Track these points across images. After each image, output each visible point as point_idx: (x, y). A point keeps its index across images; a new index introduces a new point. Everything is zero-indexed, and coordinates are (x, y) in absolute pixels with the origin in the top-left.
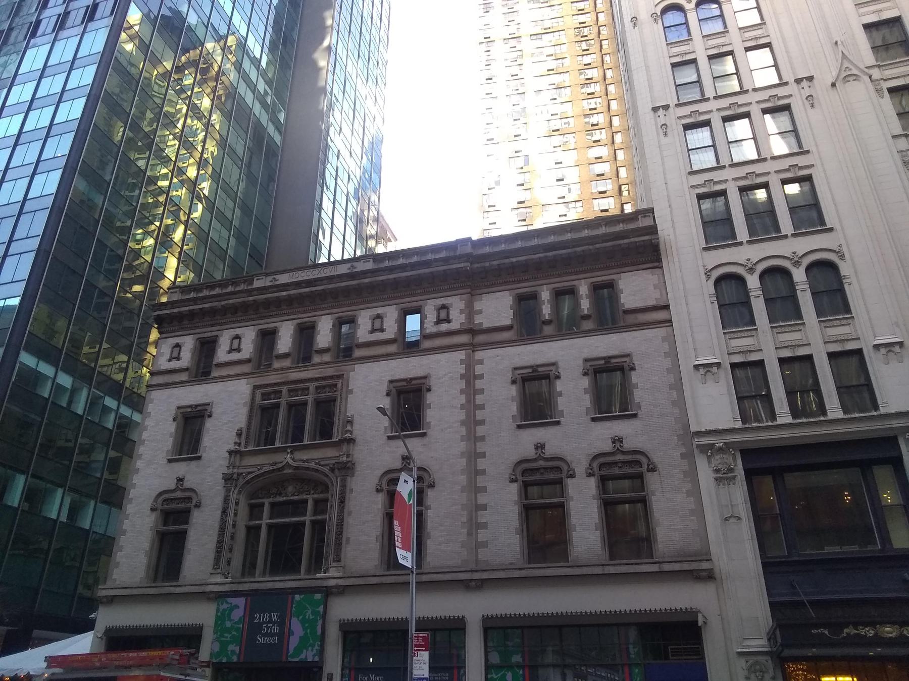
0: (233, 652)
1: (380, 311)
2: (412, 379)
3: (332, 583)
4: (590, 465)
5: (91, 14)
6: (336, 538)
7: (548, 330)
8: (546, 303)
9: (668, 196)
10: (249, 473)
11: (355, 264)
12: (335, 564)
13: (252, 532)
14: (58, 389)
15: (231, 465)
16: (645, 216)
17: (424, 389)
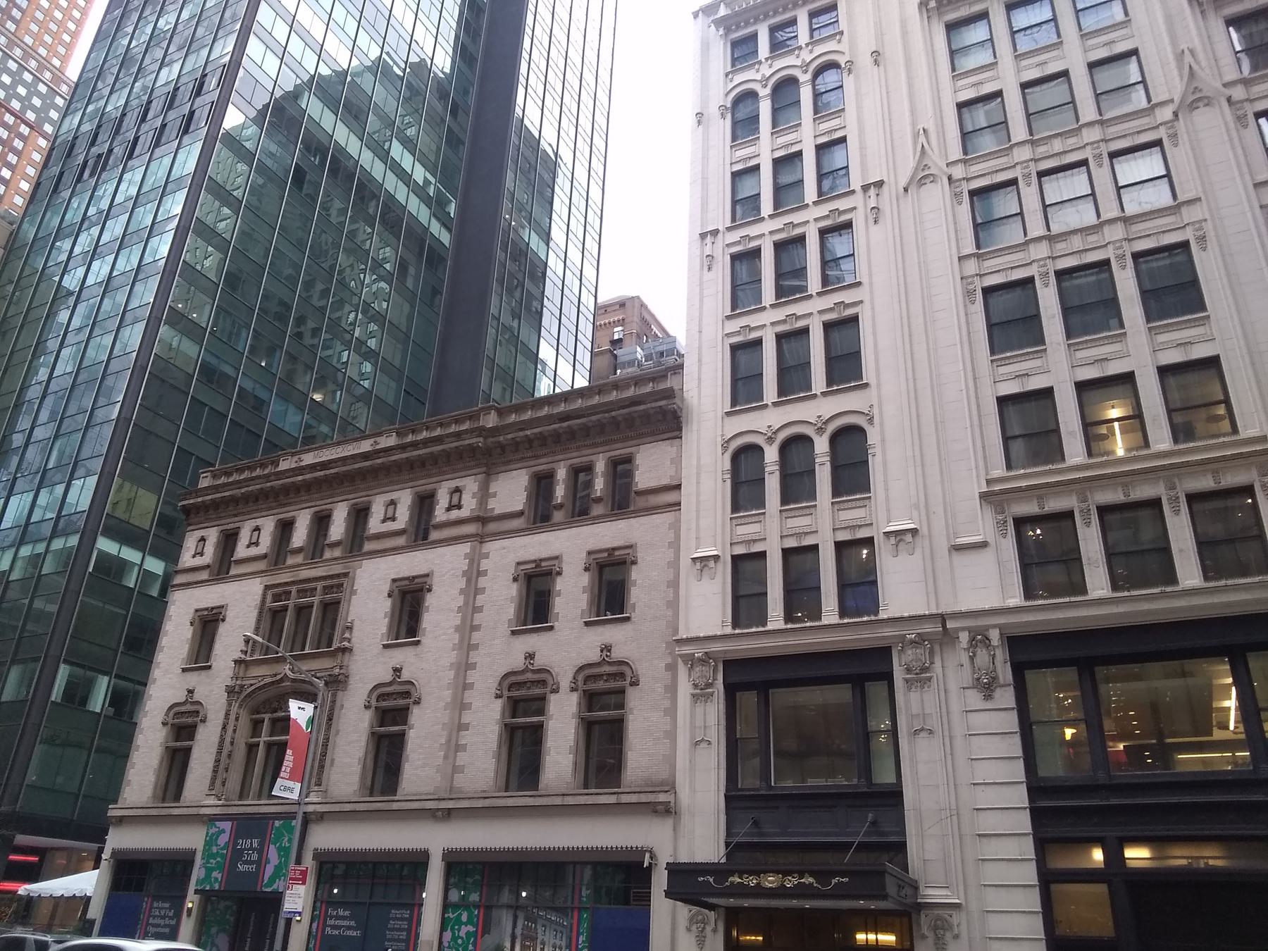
2: (414, 578)
4: (574, 679)
5: (187, 126)
6: (320, 760)
7: (597, 510)
8: (561, 483)
9: (700, 348)
10: (252, 685)
12: (316, 788)
13: (252, 748)
14: (147, 576)
15: (236, 677)
16: (675, 373)
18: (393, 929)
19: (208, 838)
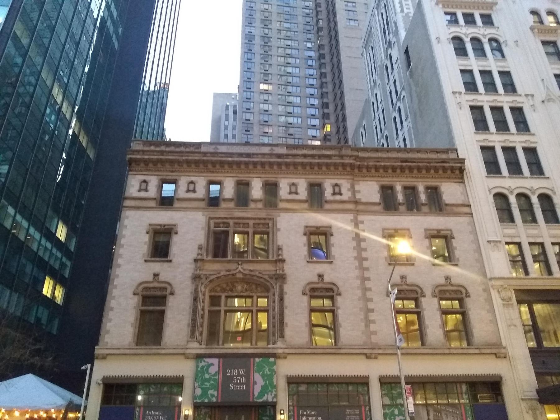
0: (213, 396)
2: (320, 227)
3: (280, 351)
8: (399, 192)
10: (210, 275)
11: (274, 148)
12: (281, 339)
17: (328, 235)
19: (199, 369)
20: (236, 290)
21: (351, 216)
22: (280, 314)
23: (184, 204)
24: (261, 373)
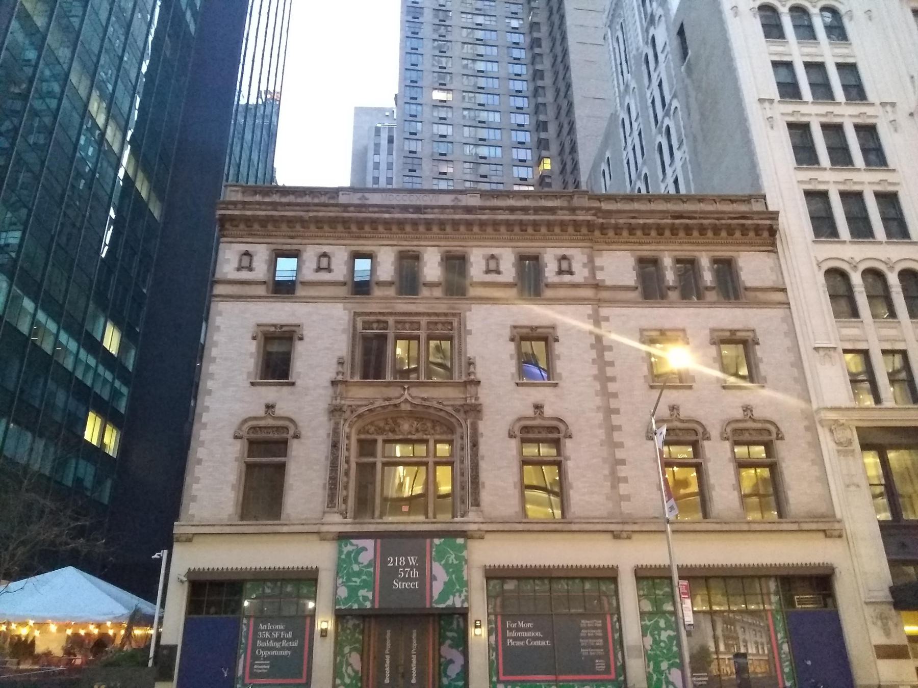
0: (365, 598)
1: (495, 251)
2: (537, 327)
8: (669, 268)
11: (460, 197)
17: (551, 339)
18: (587, 637)
19: (343, 557)
20: (400, 431)
21: (588, 309)
22: (472, 469)
23: (313, 292)
24: (443, 562)
